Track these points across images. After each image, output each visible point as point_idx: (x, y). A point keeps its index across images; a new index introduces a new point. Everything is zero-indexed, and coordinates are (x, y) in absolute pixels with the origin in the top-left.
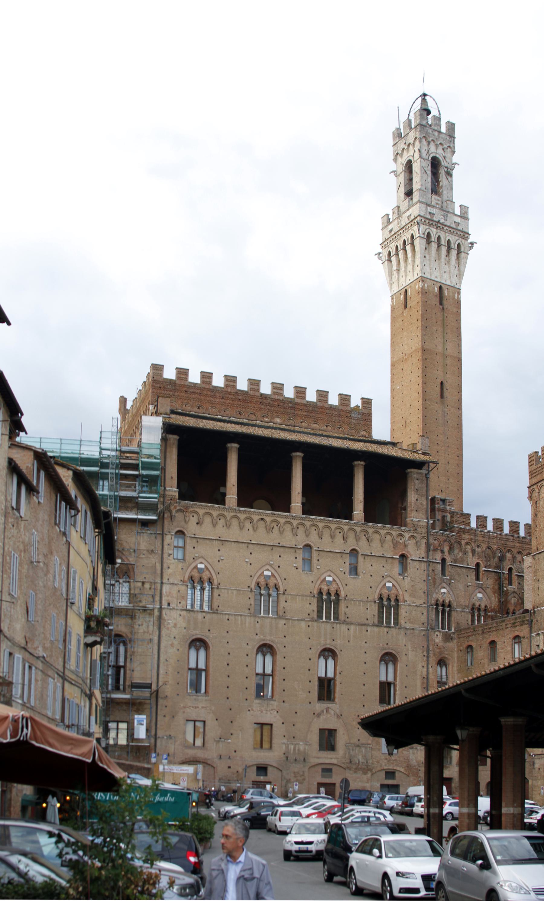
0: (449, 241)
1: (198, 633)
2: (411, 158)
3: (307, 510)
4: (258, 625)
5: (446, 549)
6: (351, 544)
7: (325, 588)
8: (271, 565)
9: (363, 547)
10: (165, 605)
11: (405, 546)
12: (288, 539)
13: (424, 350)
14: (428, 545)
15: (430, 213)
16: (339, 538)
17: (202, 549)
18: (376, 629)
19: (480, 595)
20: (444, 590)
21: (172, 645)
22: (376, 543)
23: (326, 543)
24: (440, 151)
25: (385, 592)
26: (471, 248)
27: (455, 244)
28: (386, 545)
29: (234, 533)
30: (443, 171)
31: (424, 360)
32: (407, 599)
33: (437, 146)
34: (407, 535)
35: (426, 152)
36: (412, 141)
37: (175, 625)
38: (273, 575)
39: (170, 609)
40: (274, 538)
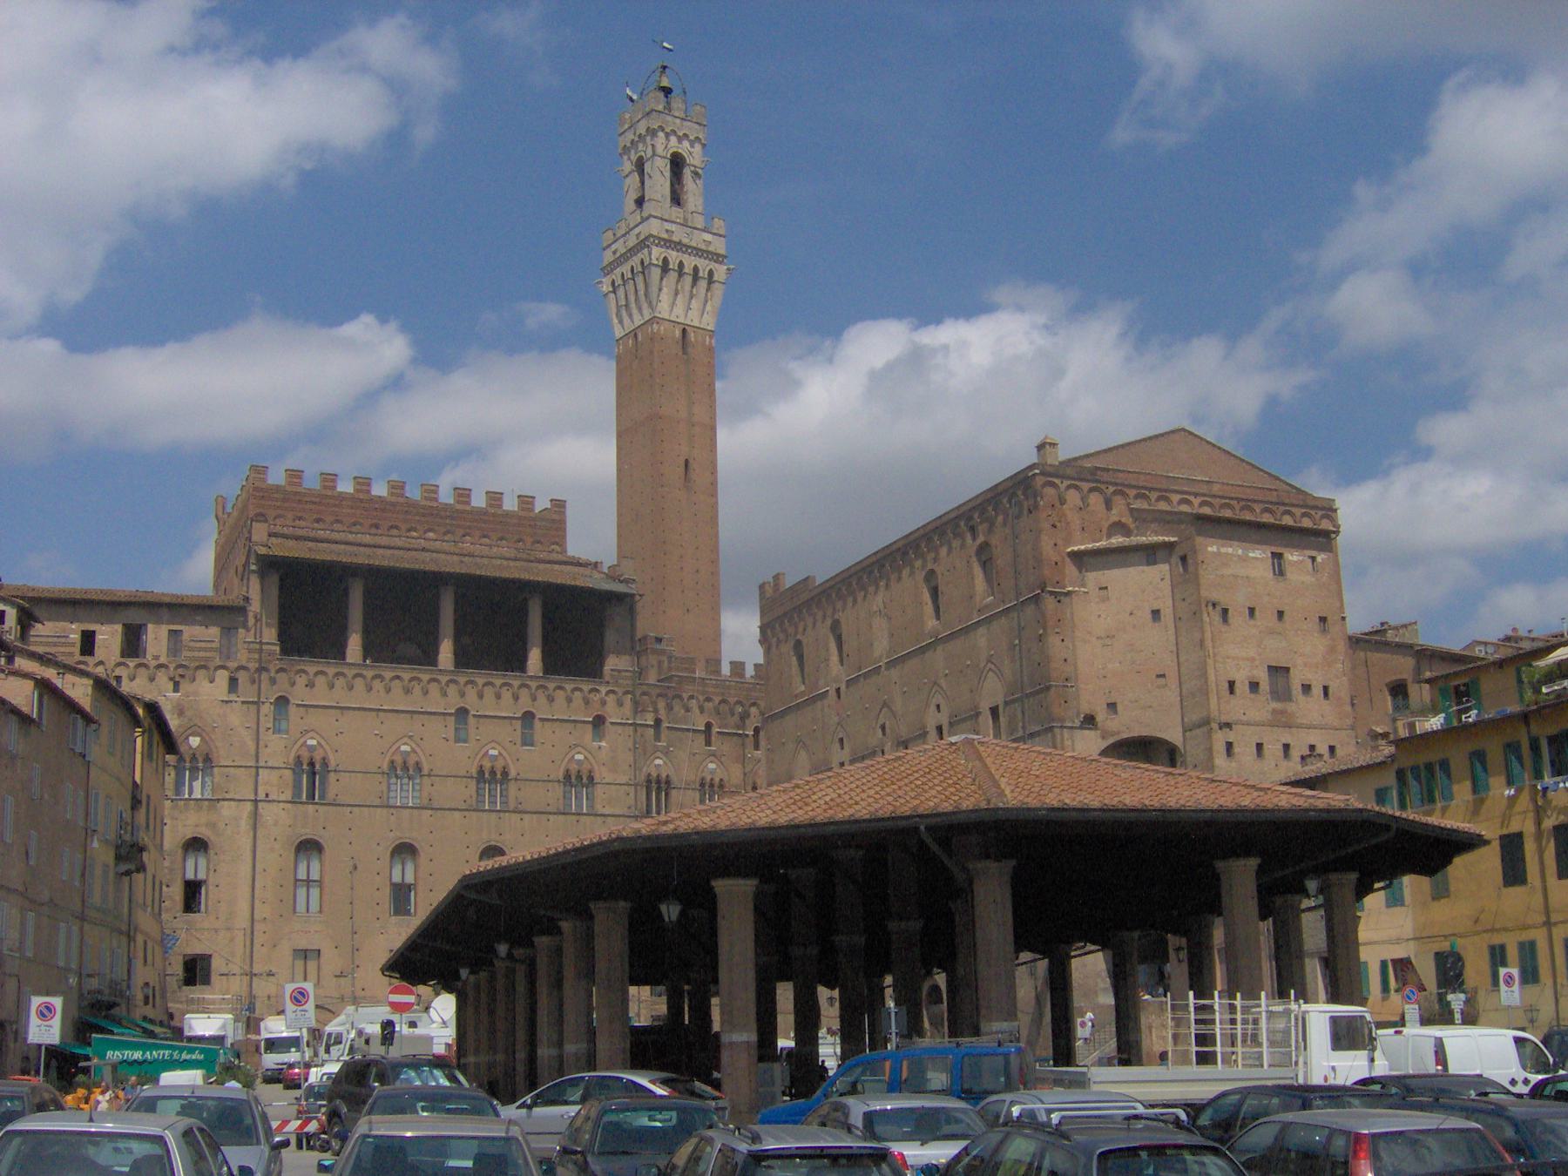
1: (307, 833)
2: (643, 154)
3: (464, 659)
4: (392, 818)
5: (661, 705)
6: (525, 703)
7: (487, 765)
8: (410, 737)
9: (542, 709)
10: (261, 796)
11: (604, 703)
12: (435, 702)
14: (636, 703)
15: (667, 231)
16: (507, 695)
17: (314, 719)
19: (712, 766)
20: (658, 762)
21: (272, 850)
24: (686, 144)
25: (574, 768)
27: (704, 271)
28: (574, 705)
29: (358, 697)
30: (689, 171)
32: (602, 774)
33: (680, 140)
35: (663, 146)
36: (643, 132)
37: (276, 824)
38: (414, 751)
39: (269, 801)
40: (415, 701)
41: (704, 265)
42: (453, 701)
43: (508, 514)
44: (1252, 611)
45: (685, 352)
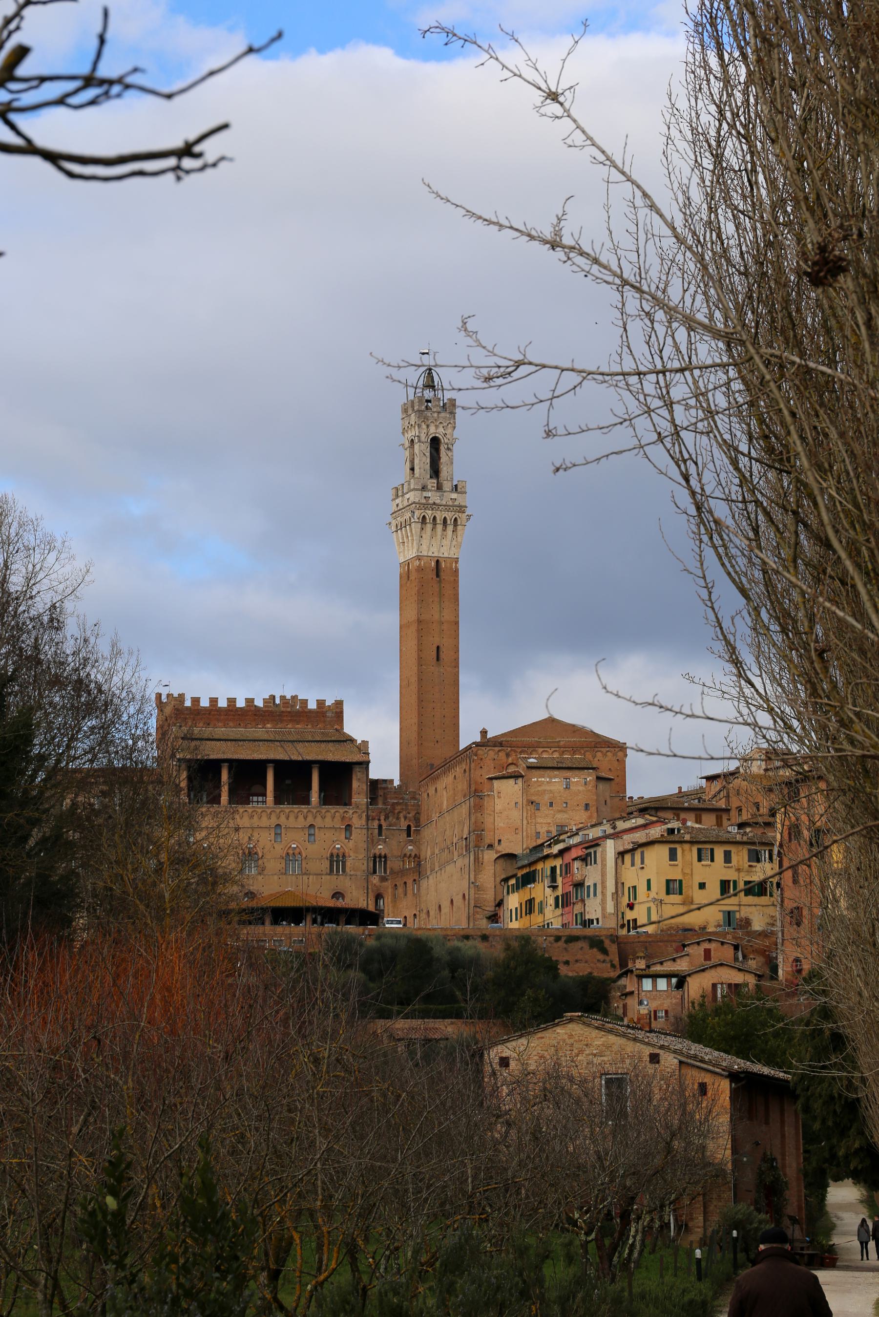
0: (445, 518)
3: (278, 801)
5: (382, 818)
6: (310, 820)
9: (318, 822)
13: (419, 621)
14: (368, 817)
16: (301, 818)
18: (328, 877)
19: (410, 847)
20: (380, 847)
22: (328, 819)
23: (292, 822)
24: (441, 430)
25: (335, 852)
26: (468, 520)
28: (335, 820)
31: (419, 631)
34: (351, 812)
41: (449, 516)
42: (274, 821)
43: (311, 711)
44: (551, 804)
45: (438, 575)
